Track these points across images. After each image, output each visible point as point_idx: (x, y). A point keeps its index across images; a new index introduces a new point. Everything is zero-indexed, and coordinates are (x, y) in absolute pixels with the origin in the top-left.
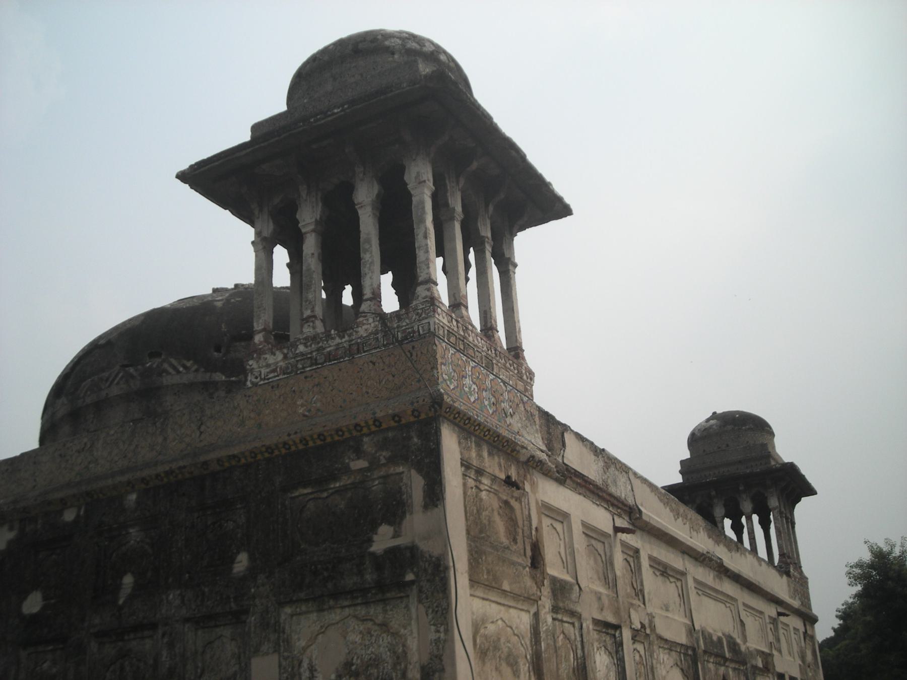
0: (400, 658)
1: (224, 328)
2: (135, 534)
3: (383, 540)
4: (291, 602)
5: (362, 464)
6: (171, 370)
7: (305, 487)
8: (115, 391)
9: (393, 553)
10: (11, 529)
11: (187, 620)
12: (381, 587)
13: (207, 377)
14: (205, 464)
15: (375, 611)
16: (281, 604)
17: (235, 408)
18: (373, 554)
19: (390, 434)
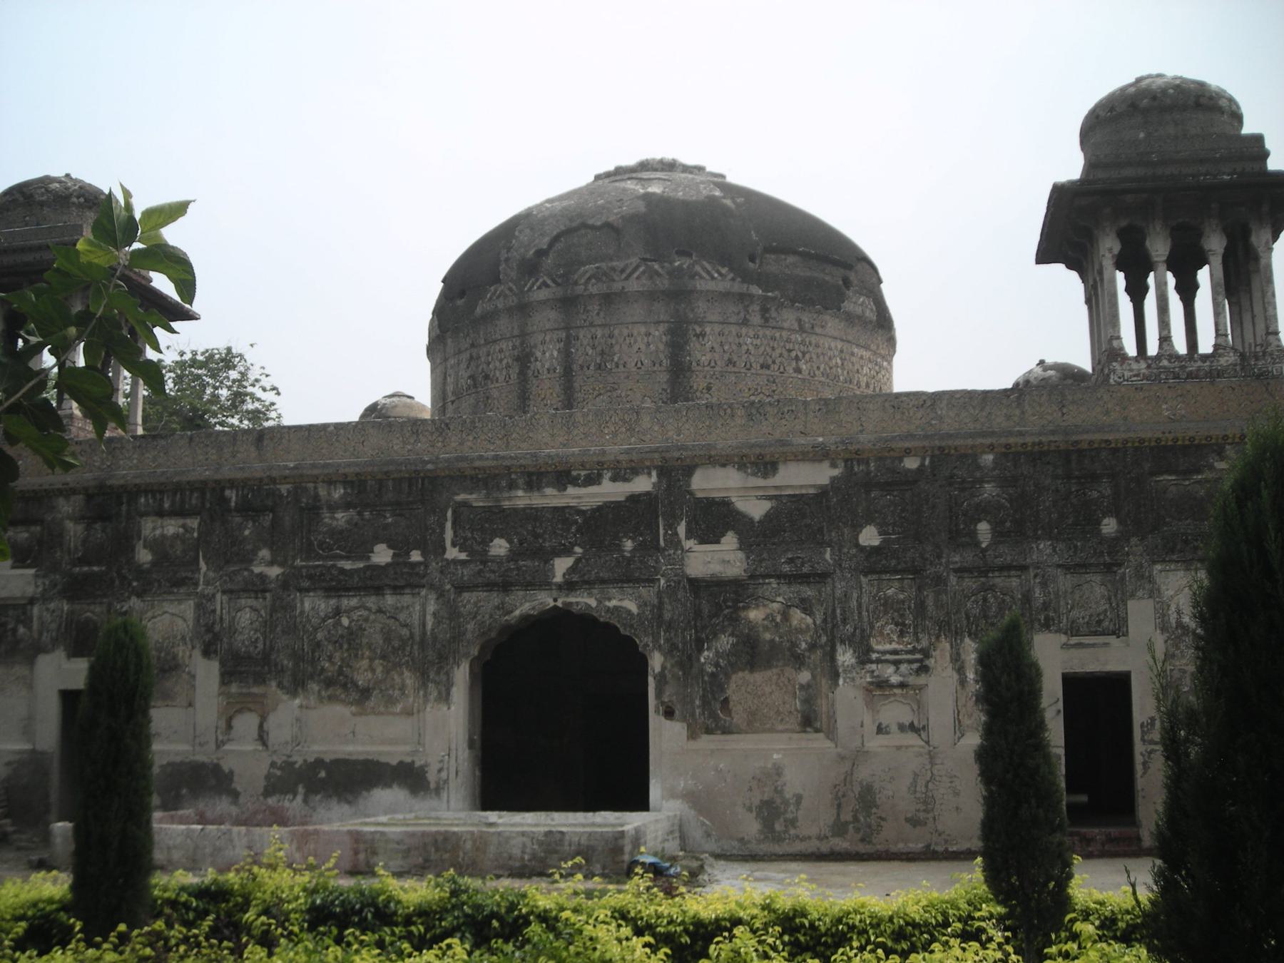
1: (754, 236)
2: (989, 490)
4: (1164, 561)
6: (704, 275)
8: (633, 285)
10: (834, 465)
11: (1059, 566)
13: (744, 288)
14: (1076, 442)
16: (1154, 562)
17: (1098, 399)
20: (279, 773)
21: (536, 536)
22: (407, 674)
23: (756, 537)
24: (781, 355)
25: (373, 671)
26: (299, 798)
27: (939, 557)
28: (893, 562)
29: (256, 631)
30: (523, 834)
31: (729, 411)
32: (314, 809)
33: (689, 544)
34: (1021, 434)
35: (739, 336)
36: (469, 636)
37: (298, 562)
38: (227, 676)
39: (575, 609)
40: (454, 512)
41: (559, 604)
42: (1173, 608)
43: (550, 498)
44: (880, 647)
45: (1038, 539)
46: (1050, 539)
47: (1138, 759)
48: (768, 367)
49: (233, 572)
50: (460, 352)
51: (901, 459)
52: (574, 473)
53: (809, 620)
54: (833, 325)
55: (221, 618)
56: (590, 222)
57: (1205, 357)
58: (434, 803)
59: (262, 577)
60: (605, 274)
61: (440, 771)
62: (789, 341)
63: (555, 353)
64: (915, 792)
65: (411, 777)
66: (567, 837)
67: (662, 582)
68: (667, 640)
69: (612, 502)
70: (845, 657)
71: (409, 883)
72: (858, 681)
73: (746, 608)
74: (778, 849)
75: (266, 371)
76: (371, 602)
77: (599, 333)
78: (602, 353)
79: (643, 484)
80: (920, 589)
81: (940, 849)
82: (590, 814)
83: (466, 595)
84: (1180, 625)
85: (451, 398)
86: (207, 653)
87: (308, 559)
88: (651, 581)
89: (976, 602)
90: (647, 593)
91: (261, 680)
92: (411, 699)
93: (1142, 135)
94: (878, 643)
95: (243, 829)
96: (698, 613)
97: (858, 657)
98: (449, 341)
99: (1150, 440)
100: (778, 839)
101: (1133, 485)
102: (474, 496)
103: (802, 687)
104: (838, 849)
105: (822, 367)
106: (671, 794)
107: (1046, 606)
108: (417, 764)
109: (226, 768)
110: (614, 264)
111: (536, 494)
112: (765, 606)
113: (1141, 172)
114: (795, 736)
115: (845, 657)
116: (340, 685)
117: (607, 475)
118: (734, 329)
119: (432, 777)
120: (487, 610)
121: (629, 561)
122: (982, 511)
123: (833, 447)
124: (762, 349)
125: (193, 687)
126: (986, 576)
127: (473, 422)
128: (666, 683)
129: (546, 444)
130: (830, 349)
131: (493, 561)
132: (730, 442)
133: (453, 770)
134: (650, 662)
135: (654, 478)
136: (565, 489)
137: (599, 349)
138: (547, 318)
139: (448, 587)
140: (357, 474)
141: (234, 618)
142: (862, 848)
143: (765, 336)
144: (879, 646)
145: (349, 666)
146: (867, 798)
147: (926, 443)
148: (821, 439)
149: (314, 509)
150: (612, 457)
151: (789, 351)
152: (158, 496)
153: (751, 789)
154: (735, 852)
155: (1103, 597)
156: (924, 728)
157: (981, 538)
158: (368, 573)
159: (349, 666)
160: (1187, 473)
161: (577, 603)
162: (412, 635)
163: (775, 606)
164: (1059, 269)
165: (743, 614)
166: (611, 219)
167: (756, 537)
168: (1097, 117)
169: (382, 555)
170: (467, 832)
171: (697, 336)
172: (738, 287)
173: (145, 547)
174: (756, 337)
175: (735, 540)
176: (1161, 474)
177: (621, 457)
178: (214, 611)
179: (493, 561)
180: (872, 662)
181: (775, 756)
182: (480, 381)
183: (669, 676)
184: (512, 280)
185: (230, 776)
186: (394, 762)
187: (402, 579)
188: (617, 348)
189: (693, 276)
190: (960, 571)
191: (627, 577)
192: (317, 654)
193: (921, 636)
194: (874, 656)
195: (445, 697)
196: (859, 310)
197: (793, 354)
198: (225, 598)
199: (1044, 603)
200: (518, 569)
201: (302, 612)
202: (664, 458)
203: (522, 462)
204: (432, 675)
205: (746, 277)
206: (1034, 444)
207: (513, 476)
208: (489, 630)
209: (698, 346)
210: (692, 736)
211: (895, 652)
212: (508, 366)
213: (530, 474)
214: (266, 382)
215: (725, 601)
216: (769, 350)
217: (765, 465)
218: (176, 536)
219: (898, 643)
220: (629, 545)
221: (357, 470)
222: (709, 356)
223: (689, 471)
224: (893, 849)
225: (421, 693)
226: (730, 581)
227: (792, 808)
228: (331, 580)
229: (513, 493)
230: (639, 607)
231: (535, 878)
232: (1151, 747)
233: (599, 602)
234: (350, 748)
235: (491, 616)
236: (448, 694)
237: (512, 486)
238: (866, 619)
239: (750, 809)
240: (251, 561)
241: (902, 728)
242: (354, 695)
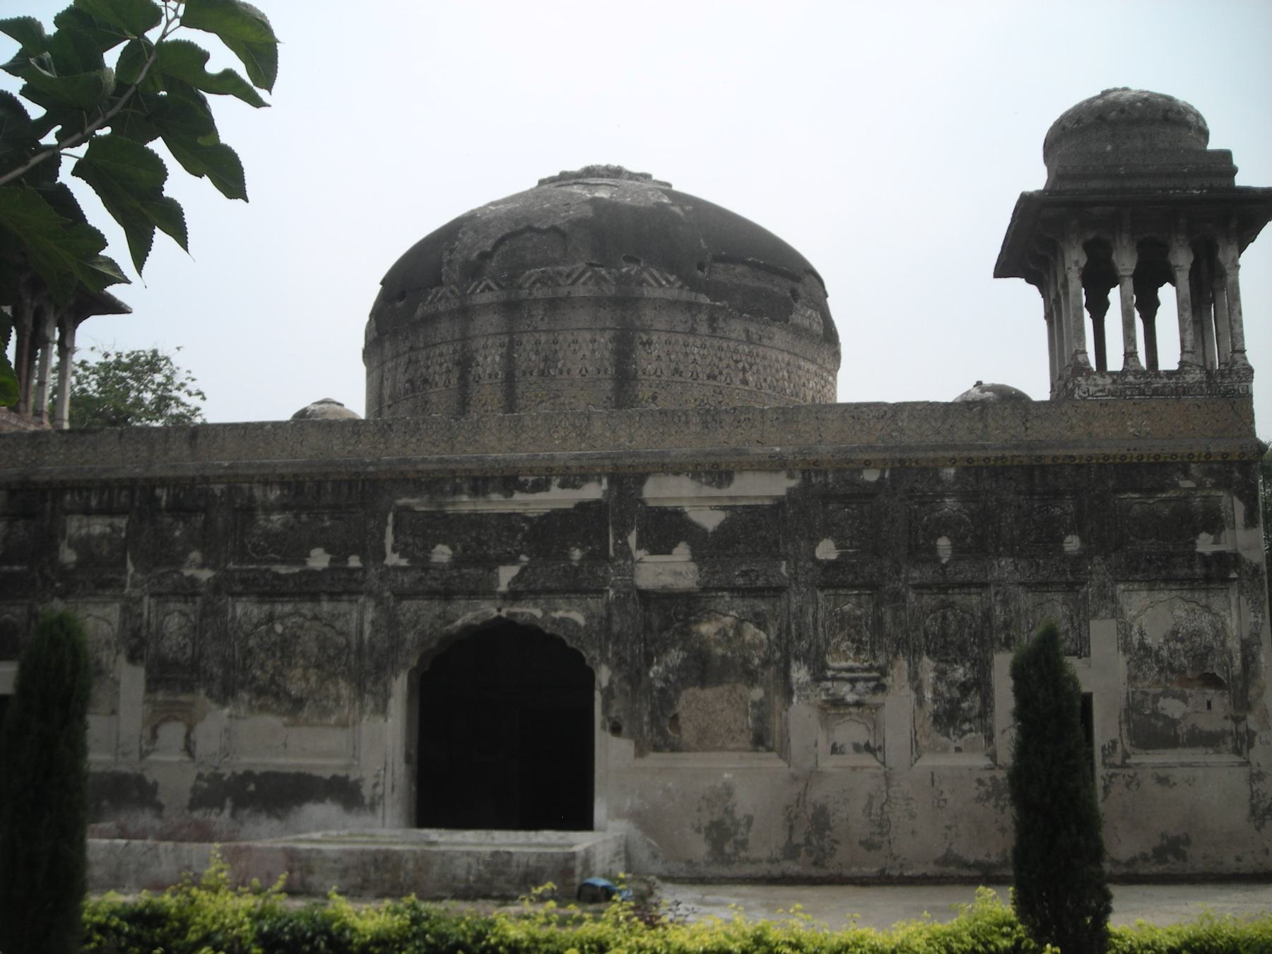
0: (1220, 632)
1: (704, 246)
3: (1205, 544)
4: (1127, 581)
5: (1189, 484)
6: (652, 282)
7: (1134, 492)
8: (580, 291)
9: (1220, 556)
10: (791, 476)
11: (1020, 584)
12: (1208, 579)
14: (1040, 457)
15: (1200, 596)
16: (1117, 581)
18: (1201, 554)
19: (1215, 466)
20: (205, 785)
22: (342, 684)
23: (708, 548)
24: (728, 366)
25: (307, 680)
26: (227, 812)
27: (898, 573)
28: (851, 577)
29: (185, 636)
30: (468, 854)
31: (683, 418)
32: (242, 824)
33: (639, 554)
34: (984, 447)
35: (686, 345)
36: (408, 645)
37: (231, 566)
38: (153, 683)
39: (519, 620)
40: (395, 517)
41: (503, 613)
42: (1136, 629)
43: (496, 504)
44: (836, 665)
45: (1000, 556)
46: (1012, 555)
47: (1099, 783)
48: (715, 378)
49: (162, 574)
50: (398, 355)
51: (860, 471)
52: (522, 479)
53: (763, 635)
54: (780, 337)
55: (148, 623)
56: (536, 225)
57: (1170, 374)
58: (367, 819)
59: (193, 580)
60: (550, 278)
61: (376, 785)
62: (736, 351)
63: (497, 358)
64: (870, 814)
65: (345, 792)
66: (515, 858)
67: (611, 593)
68: (616, 654)
69: (560, 510)
70: (800, 674)
71: (367, 907)
72: (812, 699)
73: (697, 622)
74: (726, 872)
75: (192, 375)
76: (307, 608)
77: (543, 338)
78: (546, 359)
79: (593, 491)
80: (877, 605)
81: (895, 873)
82: (532, 834)
83: (406, 604)
84: (1143, 646)
85: (387, 402)
86: (133, 658)
88: (601, 592)
89: (935, 619)
91: (188, 687)
92: (346, 711)
93: (1109, 148)
94: (834, 660)
95: (170, 844)
97: (813, 674)
98: (387, 344)
99: (1115, 457)
100: (728, 861)
101: (1096, 502)
102: (416, 500)
103: (754, 704)
104: (789, 872)
105: (769, 379)
106: (618, 814)
107: (1007, 625)
108: (352, 778)
109: (150, 779)
110: (561, 268)
111: (481, 499)
112: (717, 620)
113: (1108, 184)
114: (746, 754)
115: (800, 674)
116: (272, 695)
117: (556, 481)
118: (680, 338)
119: (366, 791)
120: (425, 618)
121: (577, 570)
122: (943, 526)
123: (791, 458)
124: (708, 360)
125: (117, 694)
126: (946, 593)
127: (417, 423)
129: (493, 448)
130: (777, 361)
131: (435, 569)
132: (684, 450)
133: (389, 785)
134: (598, 677)
135: (605, 485)
136: (512, 495)
137: (542, 355)
138: (488, 323)
139: (387, 594)
140: (295, 475)
141: (162, 622)
142: (814, 872)
143: (712, 346)
144: (835, 663)
145: (281, 674)
146: (821, 820)
147: (887, 455)
148: (778, 449)
149: (249, 510)
151: (737, 362)
152: (85, 494)
153: (699, 810)
154: (683, 874)
155: (1065, 616)
156: (880, 748)
157: (941, 553)
158: (304, 579)
159: (281, 674)
160: (1151, 491)
161: (523, 614)
162: (348, 645)
163: (728, 620)
164: (1019, 284)
165: (694, 628)
166: (558, 223)
167: (708, 548)
168: (1064, 128)
169: (319, 560)
170: (409, 851)
171: (644, 344)
172: (686, 295)
173: (70, 546)
174: (703, 346)
175: (688, 551)
176: (1125, 492)
177: (570, 463)
178: (141, 615)
179: (435, 569)
180: (827, 679)
181: (726, 775)
182: (418, 385)
183: (616, 691)
184: (454, 283)
185: (154, 788)
186: (327, 775)
187: (340, 585)
188: (560, 355)
189: (641, 283)
190: (920, 587)
191: (575, 588)
192: (248, 662)
193: (878, 653)
194: (830, 673)
195: (382, 709)
196: (806, 323)
197: (740, 365)
198: (153, 601)
199: (1005, 622)
200: (461, 576)
201: (234, 618)
202: (615, 465)
203: (468, 466)
204: (369, 685)
205: (695, 285)
206: (997, 458)
209: (644, 355)
210: (640, 753)
211: (851, 670)
212: (448, 371)
213: (475, 479)
214: (192, 386)
216: (716, 361)
217: (720, 474)
218: (103, 536)
219: (855, 661)
220: (577, 554)
222: (655, 365)
223: (641, 479)
224: (846, 873)
227: (742, 829)
229: (457, 498)
230: (587, 618)
231: (480, 901)
232: (1112, 771)
233: (545, 613)
234: (282, 761)
235: (432, 626)
237: (457, 490)
238: (821, 635)
239: (698, 830)
240: (182, 563)
241: (857, 748)
242: (287, 705)
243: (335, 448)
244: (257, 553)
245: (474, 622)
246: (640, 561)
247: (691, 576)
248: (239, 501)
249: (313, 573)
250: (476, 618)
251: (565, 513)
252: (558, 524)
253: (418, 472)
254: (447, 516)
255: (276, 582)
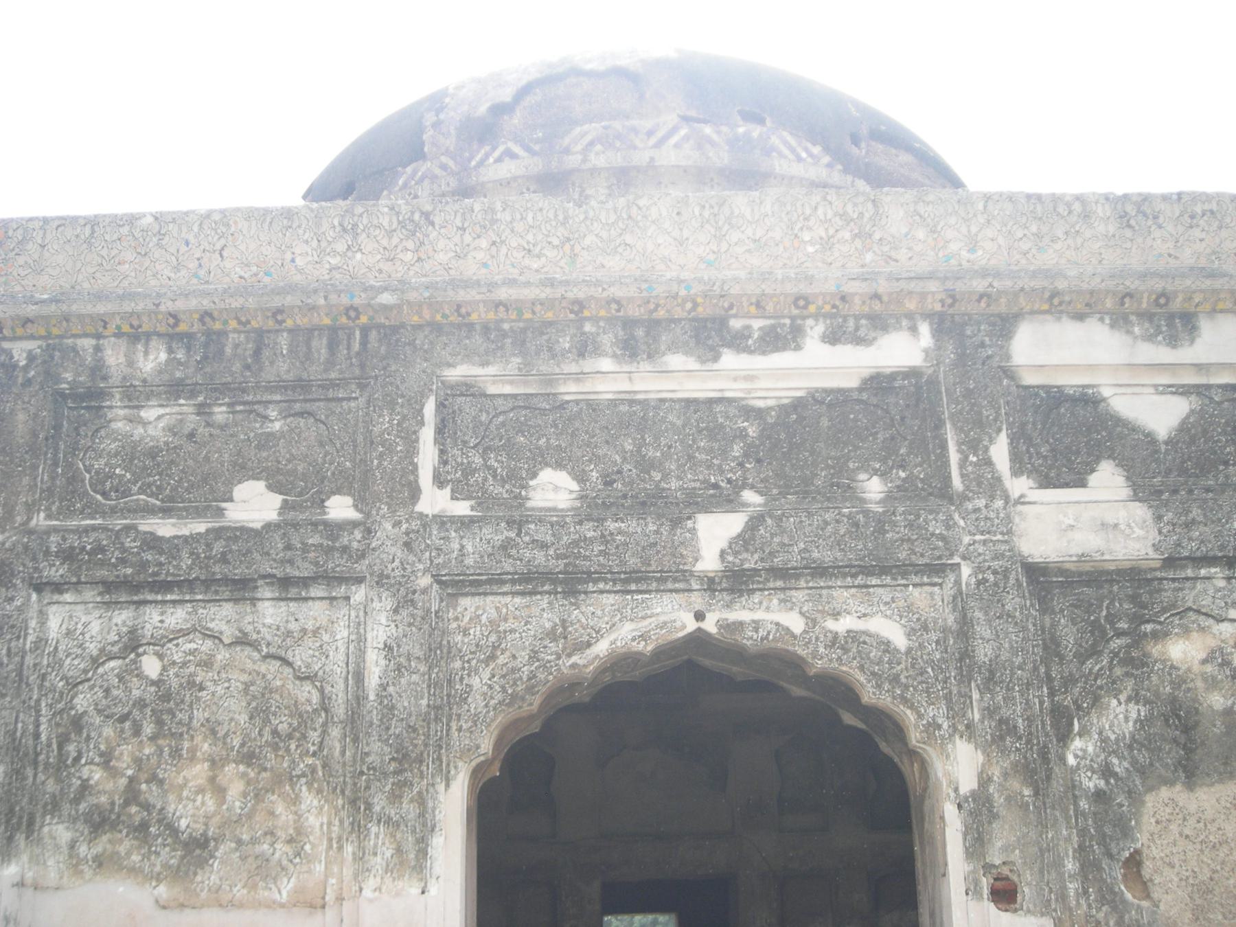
6: (786, 152)
8: (669, 156)
21: (646, 466)
22: (309, 799)
25: (220, 792)
33: (1019, 486)
36: (476, 703)
37: (40, 520)
39: (749, 639)
40: (440, 406)
43: (679, 377)
52: (736, 324)
67: (966, 571)
68: (989, 712)
69: (828, 391)
76: (223, 617)
79: (903, 351)
83: (468, 604)
87: (67, 512)
90: (930, 600)
92: (319, 868)
96: (1052, 648)
102: (491, 370)
111: (645, 366)
112: (1202, 629)
121: (882, 523)
128: (994, 816)
134: (939, 768)
136: (716, 358)
139: (425, 581)
140: (206, 315)
150: (831, 287)
158: (218, 547)
161: (757, 625)
162: (325, 706)
165: (1155, 650)
169: (254, 504)
177: (852, 287)
183: (999, 800)
184: (447, 152)
189: (768, 151)
191: (879, 564)
192: (71, 748)
195: (414, 861)
201: (41, 642)
203: (617, 292)
204: (379, 803)
207: (588, 327)
208: (530, 690)
213: (629, 324)
215: (1111, 619)
220: (874, 488)
221: (206, 304)
223: (1004, 326)
225: (349, 849)
226: (1119, 572)
228: (122, 561)
229: (589, 365)
230: (908, 635)
233: (812, 622)
235: (534, 656)
236: (423, 853)
237: (585, 348)
242: (167, 856)
243: (300, 262)
244: (104, 494)
245: (640, 647)
246: (1021, 501)
247: (1139, 532)
248: (69, 376)
249: (243, 532)
250: (644, 637)
251: (835, 400)
252: (825, 423)
253: (498, 304)
254: (563, 406)
255: (148, 556)
